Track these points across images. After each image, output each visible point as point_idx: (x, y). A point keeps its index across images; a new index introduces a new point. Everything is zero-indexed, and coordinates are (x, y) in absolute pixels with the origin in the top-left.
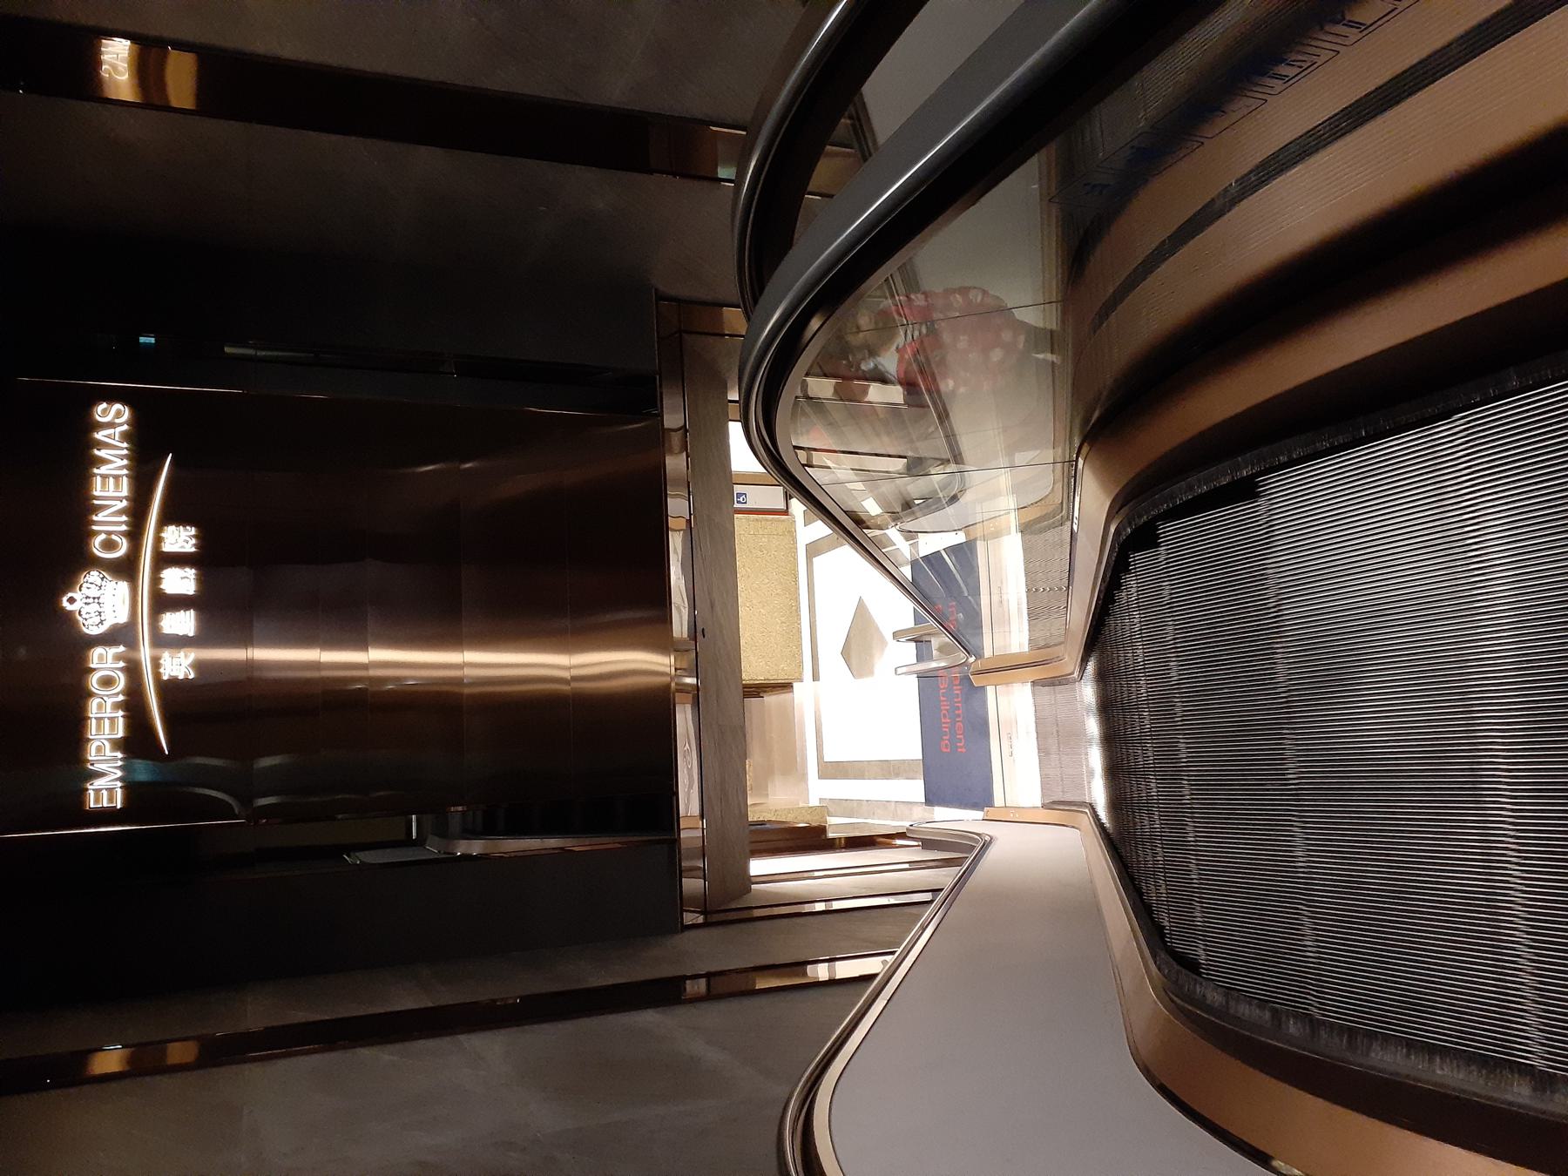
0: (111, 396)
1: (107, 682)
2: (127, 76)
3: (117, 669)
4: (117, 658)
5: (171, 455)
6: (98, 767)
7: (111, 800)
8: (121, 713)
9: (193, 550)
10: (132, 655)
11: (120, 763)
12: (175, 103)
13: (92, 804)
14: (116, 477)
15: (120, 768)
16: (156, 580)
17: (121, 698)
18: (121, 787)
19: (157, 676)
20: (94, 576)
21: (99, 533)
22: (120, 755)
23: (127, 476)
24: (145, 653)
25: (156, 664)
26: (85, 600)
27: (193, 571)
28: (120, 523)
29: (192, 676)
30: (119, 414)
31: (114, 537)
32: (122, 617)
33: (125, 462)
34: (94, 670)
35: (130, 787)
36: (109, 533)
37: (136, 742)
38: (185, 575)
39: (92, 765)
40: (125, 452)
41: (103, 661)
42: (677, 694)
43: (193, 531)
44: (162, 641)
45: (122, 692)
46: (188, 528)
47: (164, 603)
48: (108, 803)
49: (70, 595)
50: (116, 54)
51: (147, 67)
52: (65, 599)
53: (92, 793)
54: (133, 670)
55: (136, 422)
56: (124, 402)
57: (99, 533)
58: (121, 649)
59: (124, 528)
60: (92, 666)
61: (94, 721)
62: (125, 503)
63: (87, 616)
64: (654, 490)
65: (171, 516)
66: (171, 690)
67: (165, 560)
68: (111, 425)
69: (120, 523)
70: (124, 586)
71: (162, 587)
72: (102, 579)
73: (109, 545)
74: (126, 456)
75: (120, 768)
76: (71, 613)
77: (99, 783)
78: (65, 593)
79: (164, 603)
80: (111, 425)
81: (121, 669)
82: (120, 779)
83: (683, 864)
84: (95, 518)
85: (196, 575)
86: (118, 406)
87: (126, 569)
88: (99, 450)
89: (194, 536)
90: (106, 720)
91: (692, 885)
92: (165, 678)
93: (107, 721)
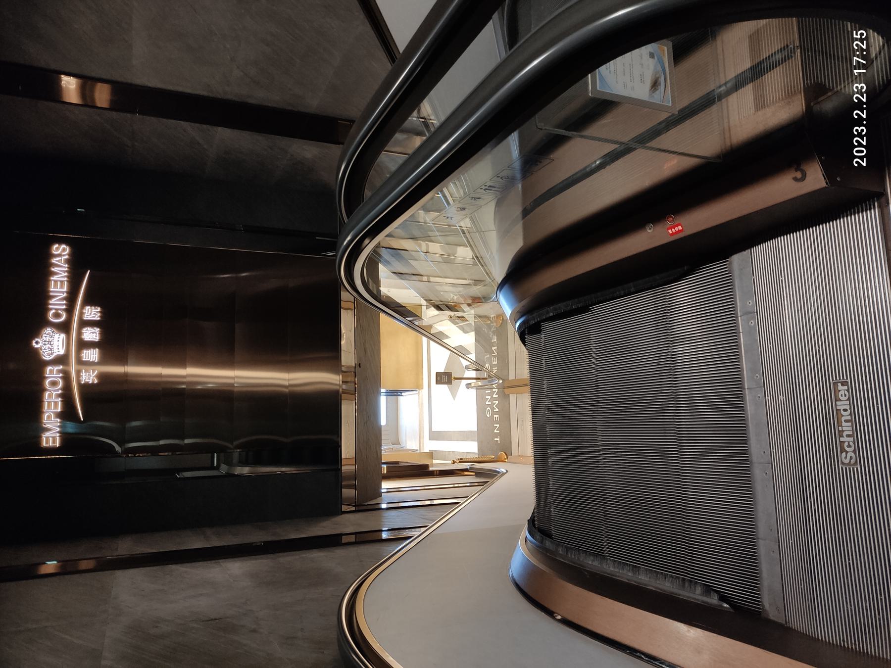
0: (60, 241)
1: (54, 384)
2: (75, 86)
3: (58, 377)
4: (59, 371)
5: (89, 271)
6: (48, 426)
7: (54, 442)
8: (60, 399)
9: (99, 319)
10: (66, 368)
11: (59, 424)
12: (99, 105)
13: (44, 444)
14: (62, 282)
15: (59, 427)
16: (79, 334)
17: (60, 392)
18: (59, 436)
19: (79, 381)
20: (49, 330)
21: (52, 309)
22: (59, 420)
23: (67, 281)
24: (73, 369)
25: (78, 373)
26: (43, 343)
27: (98, 329)
28: (62, 305)
29: (96, 382)
30: (64, 250)
31: (60, 312)
32: (62, 352)
33: (66, 274)
34: (48, 377)
35: (64, 435)
36: (56, 309)
37: (68, 413)
38: (94, 331)
39: (45, 425)
40: (66, 269)
41: (52, 374)
42: (343, 395)
43: (99, 309)
44: (80, 362)
45: (61, 389)
46: (96, 308)
47: (83, 345)
48: (52, 444)
49: (36, 340)
50: (70, 84)
51: (86, 88)
52: (34, 342)
53: (44, 438)
54: (67, 378)
55: (73, 254)
56: (67, 244)
57: (52, 309)
58: (61, 367)
59: (64, 307)
60: (47, 376)
61: (46, 403)
62: (65, 295)
63: (45, 351)
64: (335, 288)
65: (90, 300)
66: (85, 389)
67: (84, 324)
68: (60, 255)
69: (62, 305)
70: (63, 336)
71: (83, 337)
72: (53, 332)
73: (57, 315)
74: (67, 271)
75: (59, 427)
76: (37, 349)
77: (48, 434)
78: (34, 339)
79: (83, 345)
80: (60, 255)
81: (61, 378)
82: (58, 432)
83: (343, 483)
84: (51, 302)
85: (100, 331)
86: (63, 246)
87: (65, 328)
88: (53, 268)
89: (100, 312)
90: (53, 403)
91: (348, 493)
92: (83, 382)
93: (53, 403)
